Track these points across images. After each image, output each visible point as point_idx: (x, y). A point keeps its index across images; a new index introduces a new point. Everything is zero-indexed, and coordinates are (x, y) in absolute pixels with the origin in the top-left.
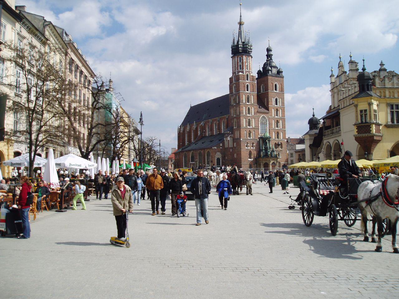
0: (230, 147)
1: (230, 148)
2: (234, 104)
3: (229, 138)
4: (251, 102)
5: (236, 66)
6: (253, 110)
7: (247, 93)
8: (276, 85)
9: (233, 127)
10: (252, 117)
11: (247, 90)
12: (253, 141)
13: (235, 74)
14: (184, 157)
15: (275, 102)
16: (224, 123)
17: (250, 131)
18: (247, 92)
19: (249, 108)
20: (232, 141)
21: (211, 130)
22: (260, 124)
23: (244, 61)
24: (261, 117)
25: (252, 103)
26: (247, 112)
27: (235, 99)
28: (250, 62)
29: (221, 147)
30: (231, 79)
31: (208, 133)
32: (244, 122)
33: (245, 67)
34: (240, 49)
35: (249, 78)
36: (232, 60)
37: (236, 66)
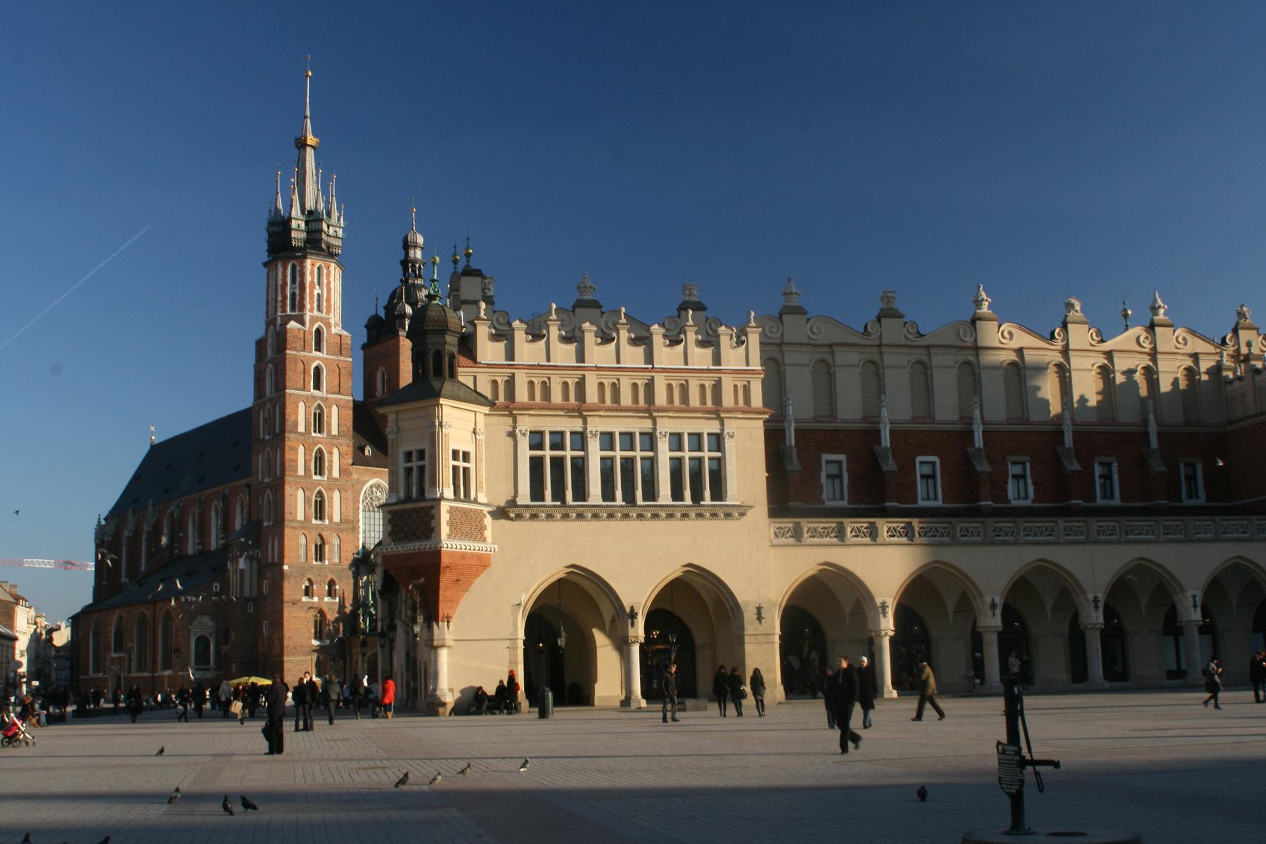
0: (247, 594)
1: (248, 600)
2: (267, 437)
3: (242, 564)
4: (329, 431)
5: (280, 298)
6: (335, 462)
7: (314, 398)
10: (333, 485)
12: (332, 572)
13: (275, 326)
16: (242, 508)
17: (320, 536)
18: (316, 393)
19: (320, 451)
20: (255, 574)
21: (203, 532)
22: (360, 511)
23: (308, 278)
24: (368, 485)
25: (335, 432)
27: (269, 421)
28: (332, 286)
30: (260, 345)
31: (194, 542)
32: (297, 504)
33: (311, 303)
34: (294, 234)
35: (324, 345)
36: (268, 274)
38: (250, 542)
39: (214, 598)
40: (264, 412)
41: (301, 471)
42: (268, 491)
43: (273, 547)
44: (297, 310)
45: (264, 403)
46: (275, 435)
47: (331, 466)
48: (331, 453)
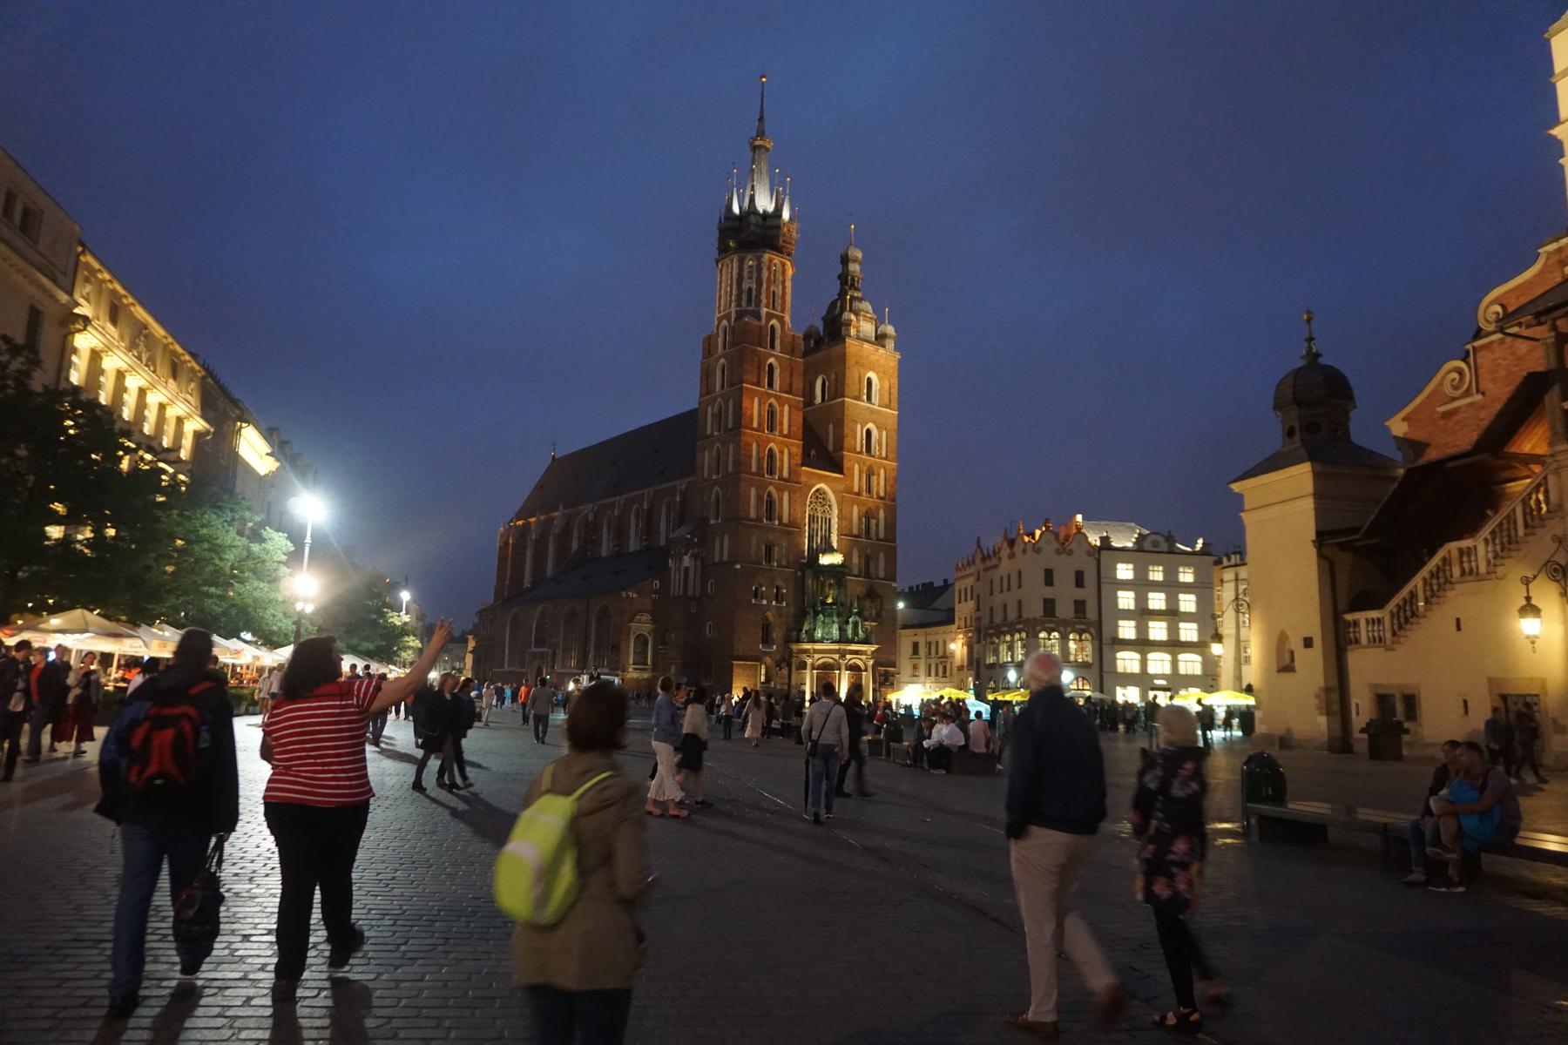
0: (690, 593)
3: (687, 561)
7: (770, 396)
8: (869, 381)
9: (705, 520)
11: (771, 385)
14: (511, 629)
15: (864, 442)
16: (668, 511)
20: (699, 573)
21: (620, 534)
24: (814, 489)
26: (765, 466)
29: (656, 592)
33: (767, 298)
35: (777, 342)
37: (734, 293)
38: (696, 540)
39: (654, 596)
40: (713, 408)
41: (754, 469)
42: (717, 488)
43: (722, 546)
44: (753, 305)
45: (715, 399)
46: (727, 430)
47: (782, 466)
48: (782, 452)
